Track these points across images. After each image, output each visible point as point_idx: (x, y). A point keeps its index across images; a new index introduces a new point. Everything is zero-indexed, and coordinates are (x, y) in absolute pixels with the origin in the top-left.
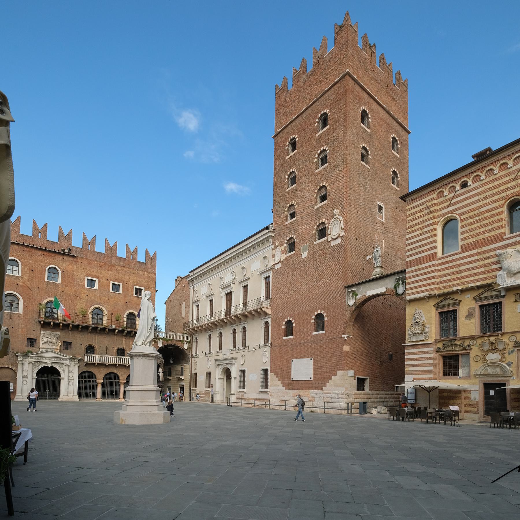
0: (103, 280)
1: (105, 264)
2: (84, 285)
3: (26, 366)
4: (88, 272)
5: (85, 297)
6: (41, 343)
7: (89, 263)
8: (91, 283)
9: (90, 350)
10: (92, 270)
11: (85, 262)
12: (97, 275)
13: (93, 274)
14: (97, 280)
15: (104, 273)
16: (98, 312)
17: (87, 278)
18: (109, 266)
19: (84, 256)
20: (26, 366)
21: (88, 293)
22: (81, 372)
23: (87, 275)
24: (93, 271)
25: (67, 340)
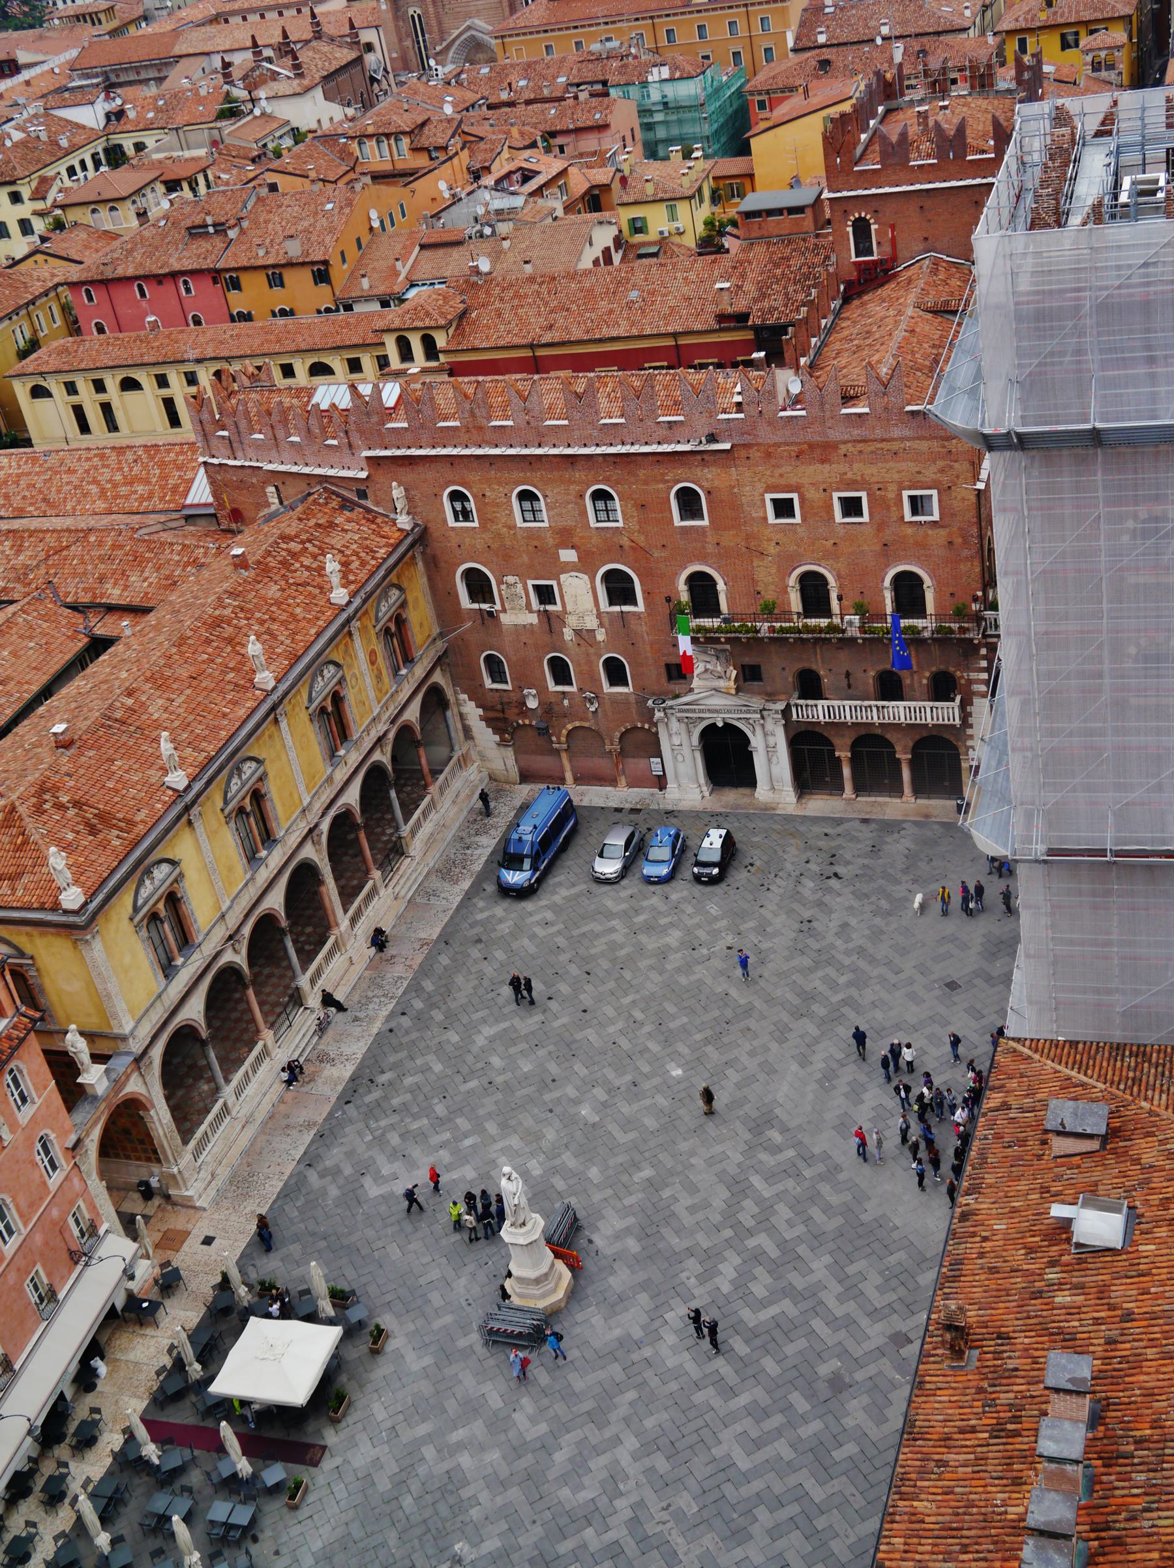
0: (812, 494)
1: (812, 446)
2: (765, 518)
3: (674, 725)
4: (771, 481)
5: (772, 549)
6: (696, 672)
7: (768, 455)
8: (783, 508)
9: (810, 687)
10: (778, 472)
11: (755, 454)
12: (793, 481)
13: (782, 482)
14: (795, 496)
15: (812, 473)
16: (814, 592)
17: (768, 497)
18: (824, 451)
19: (747, 439)
20: (674, 725)
21: (778, 537)
22: (792, 734)
23: (770, 489)
24: (781, 475)
25: (747, 660)
